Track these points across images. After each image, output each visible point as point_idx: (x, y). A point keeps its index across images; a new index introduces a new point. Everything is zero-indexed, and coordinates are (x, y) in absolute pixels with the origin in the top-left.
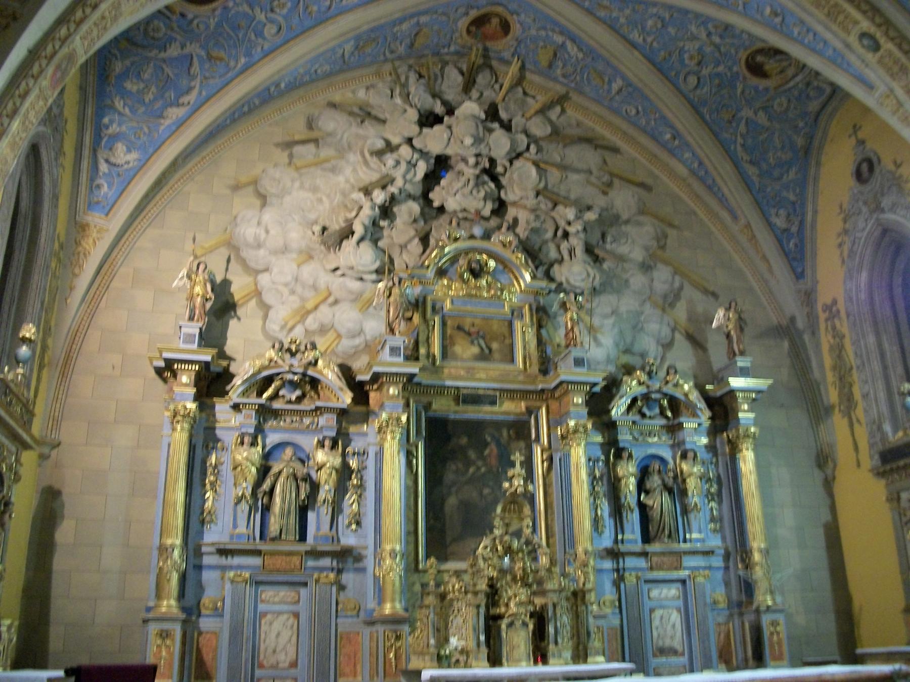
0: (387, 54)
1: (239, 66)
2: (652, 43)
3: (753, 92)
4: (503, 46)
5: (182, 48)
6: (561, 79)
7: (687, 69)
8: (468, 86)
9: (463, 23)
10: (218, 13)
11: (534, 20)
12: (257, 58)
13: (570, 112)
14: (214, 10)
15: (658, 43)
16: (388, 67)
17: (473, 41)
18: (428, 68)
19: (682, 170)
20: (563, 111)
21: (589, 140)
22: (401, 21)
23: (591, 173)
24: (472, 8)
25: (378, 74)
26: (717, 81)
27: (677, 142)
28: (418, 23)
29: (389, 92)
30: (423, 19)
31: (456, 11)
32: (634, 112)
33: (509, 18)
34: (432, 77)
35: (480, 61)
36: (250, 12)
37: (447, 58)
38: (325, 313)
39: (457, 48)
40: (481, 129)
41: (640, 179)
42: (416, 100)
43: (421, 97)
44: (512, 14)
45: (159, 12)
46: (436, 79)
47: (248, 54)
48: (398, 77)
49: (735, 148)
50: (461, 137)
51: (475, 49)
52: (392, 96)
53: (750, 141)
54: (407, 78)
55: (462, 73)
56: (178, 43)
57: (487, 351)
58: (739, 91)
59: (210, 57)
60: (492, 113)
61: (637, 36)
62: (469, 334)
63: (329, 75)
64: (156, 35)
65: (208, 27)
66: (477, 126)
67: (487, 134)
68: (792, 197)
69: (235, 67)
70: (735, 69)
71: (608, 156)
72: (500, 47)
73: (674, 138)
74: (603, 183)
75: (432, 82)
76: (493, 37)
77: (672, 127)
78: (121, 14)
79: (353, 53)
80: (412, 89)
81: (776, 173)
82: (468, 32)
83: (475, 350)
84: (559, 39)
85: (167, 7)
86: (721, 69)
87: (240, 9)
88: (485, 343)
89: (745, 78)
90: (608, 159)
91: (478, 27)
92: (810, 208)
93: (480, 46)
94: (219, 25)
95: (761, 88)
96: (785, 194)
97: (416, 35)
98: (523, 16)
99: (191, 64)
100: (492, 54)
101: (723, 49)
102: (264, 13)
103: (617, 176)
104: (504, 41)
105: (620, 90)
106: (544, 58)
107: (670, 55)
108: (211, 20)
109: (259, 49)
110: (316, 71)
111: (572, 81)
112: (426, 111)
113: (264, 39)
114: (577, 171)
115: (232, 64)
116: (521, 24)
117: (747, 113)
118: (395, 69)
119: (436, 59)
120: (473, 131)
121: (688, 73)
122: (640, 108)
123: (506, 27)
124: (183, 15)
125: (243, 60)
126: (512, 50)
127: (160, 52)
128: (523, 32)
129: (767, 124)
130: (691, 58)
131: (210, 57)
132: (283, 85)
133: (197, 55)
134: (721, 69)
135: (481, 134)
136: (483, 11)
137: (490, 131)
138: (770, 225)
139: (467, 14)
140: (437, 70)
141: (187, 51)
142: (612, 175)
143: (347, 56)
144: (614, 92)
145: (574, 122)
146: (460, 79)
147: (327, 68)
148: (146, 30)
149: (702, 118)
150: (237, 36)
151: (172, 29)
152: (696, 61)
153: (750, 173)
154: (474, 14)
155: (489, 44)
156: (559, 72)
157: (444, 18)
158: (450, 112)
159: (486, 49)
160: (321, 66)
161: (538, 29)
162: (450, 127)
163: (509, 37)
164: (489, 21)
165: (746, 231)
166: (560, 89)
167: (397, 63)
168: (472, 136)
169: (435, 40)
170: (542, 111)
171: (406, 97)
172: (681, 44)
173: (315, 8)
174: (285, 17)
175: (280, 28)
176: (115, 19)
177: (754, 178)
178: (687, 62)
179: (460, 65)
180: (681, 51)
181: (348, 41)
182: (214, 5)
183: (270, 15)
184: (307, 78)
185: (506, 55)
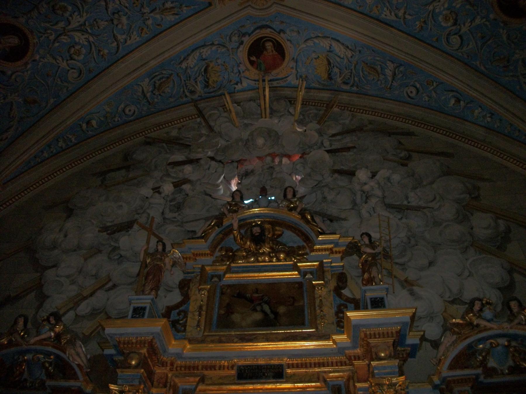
2: (405, 18)
6: (345, 87)
10: (29, 66)
24: (244, 35)
26: (479, 35)
36: (54, 62)
38: (99, 299)
44: (279, 33)
57: (272, 316)
58: (505, 38)
61: (388, 12)
62: (251, 300)
70: (492, 16)
83: (258, 316)
86: (478, 21)
87: (46, 60)
88: (270, 308)
90: (402, 141)
99: (11, 110)
102: (65, 61)
103: (412, 151)
104: (285, 64)
105: (394, 74)
107: (425, 22)
111: (352, 86)
121: (449, 35)
123: (280, 49)
130: (446, 19)
134: (478, 21)
139: (242, 43)
144: (390, 79)
154: (248, 41)
156: (339, 80)
173: (106, 51)
175: (81, 71)
178: (443, 24)
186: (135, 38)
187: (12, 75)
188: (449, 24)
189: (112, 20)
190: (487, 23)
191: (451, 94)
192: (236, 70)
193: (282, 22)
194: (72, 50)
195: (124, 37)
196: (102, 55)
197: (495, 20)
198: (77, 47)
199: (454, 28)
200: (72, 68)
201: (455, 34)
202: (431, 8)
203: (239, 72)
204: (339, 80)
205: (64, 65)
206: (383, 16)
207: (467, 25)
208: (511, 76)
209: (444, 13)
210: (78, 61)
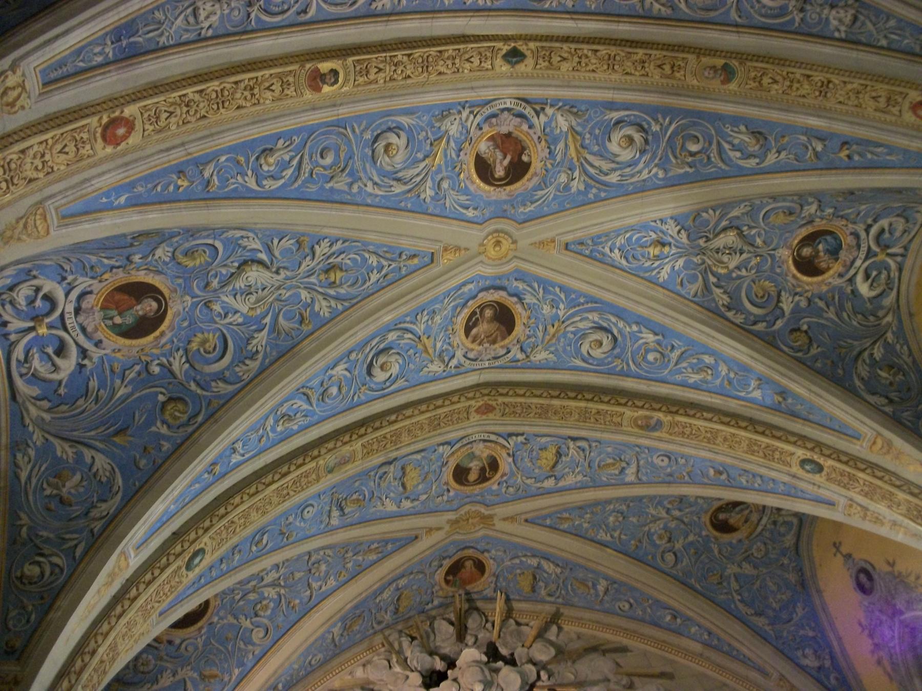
0: (375, 625)
1: (234, 678)
2: (620, 538)
3: (729, 549)
4: (483, 585)
5: (174, 675)
6: (549, 599)
7: (661, 549)
8: (461, 637)
9: (440, 575)
11: (505, 551)
12: (250, 665)
13: (566, 628)
14: (200, 629)
15: (625, 535)
16: (379, 638)
17: (453, 589)
18: (418, 628)
19: (697, 647)
20: (560, 628)
21: (594, 649)
22: (381, 590)
23: (609, 680)
24: (444, 558)
25: (371, 648)
26: (692, 551)
27: (679, 620)
28: (398, 589)
29: (386, 663)
30: (402, 582)
31: (430, 565)
32: (627, 606)
33: (481, 557)
34: (424, 635)
35: (466, 606)
36: (235, 621)
37: (434, 613)
39: (441, 600)
40: (487, 672)
41: (657, 670)
42: (415, 663)
43: (417, 657)
44: (483, 552)
45: (149, 645)
46: (428, 637)
47: (241, 664)
48: (391, 645)
49: (736, 606)
50: (470, 687)
51: (457, 596)
52: (390, 667)
53: (746, 594)
54: (400, 644)
55: (452, 623)
56: (169, 671)
58: (716, 552)
59: (203, 677)
60: (493, 653)
61: (604, 535)
63: (326, 662)
64: (146, 669)
65: (197, 648)
66: (483, 671)
67: (494, 675)
68: (811, 634)
69: (230, 680)
70: (704, 533)
71: (618, 657)
72: (481, 588)
73: (675, 617)
74: (624, 686)
75: (425, 640)
76: (472, 580)
77: (667, 607)
78: (118, 654)
79: (342, 635)
80: (408, 653)
81: (784, 615)
82: (447, 582)
84: (534, 562)
85: (156, 640)
87: (225, 621)
89: (716, 538)
90: (618, 660)
91: (455, 575)
92: (831, 636)
93: (461, 592)
94: (205, 644)
95: (734, 541)
96: (802, 632)
97: (398, 600)
98: (493, 552)
100: (475, 596)
101: (686, 520)
105: (607, 591)
106: (525, 584)
107: (640, 541)
108: (199, 640)
109: (251, 656)
110: (310, 663)
111: (558, 597)
112: (427, 671)
113: (254, 644)
114: (594, 683)
115: (226, 679)
116: (494, 559)
117: (732, 569)
118: (386, 638)
119: (423, 617)
120: (480, 677)
121: (663, 552)
122: (632, 601)
123: (480, 567)
124: (170, 642)
125: (237, 671)
126: (493, 585)
127: (152, 685)
128: (498, 566)
129: (755, 572)
130: (661, 537)
131: (203, 677)
132: (280, 686)
133: (189, 678)
134: (691, 538)
135: (489, 678)
136: (455, 558)
137: (497, 671)
138: (803, 668)
140: (427, 628)
141: (178, 677)
142: (629, 675)
143: (337, 639)
144: (601, 594)
145: (574, 636)
146: (451, 629)
147: (320, 656)
148: (135, 666)
149: (692, 588)
150: (227, 649)
151: (161, 659)
152: (666, 539)
153: (760, 625)
154: (447, 563)
155: (468, 587)
156: (543, 592)
157: (421, 576)
158: (452, 664)
159: (468, 593)
160: (314, 655)
161: (511, 559)
162: (455, 680)
163: (486, 575)
164: (463, 566)
165: (782, 683)
166: (550, 609)
167: (387, 633)
168: (480, 681)
169: (418, 600)
170: (540, 635)
171: (404, 662)
172: (647, 528)
173: (297, 601)
174: (270, 618)
176: (113, 660)
177: (767, 628)
178: (658, 542)
179: (447, 616)
180: (649, 535)
181: (334, 625)
182: (200, 624)
183: (254, 619)
184: (303, 673)
185: (489, 592)
186: (332, 582)
187: (181, 644)
188: (664, 542)
189: (310, 570)
190: (700, 539)
191: (668, 611)
192: (429, 591)
193: (488, 543)
194: (259, 606)
195: (319, 583)
196: (293, 607)
197: (707, 536)
198: (264, 603)
199: (668, 545)
200: (257, 627)
201: (669, 551)
202: (647, 528)
203: (433, 593)
204: (543, 592)
205: (247, 624)
206: (599, 537)
207: (681, 541)
208: (726, 593)
209: (659, 532)
210: (264, 617)
